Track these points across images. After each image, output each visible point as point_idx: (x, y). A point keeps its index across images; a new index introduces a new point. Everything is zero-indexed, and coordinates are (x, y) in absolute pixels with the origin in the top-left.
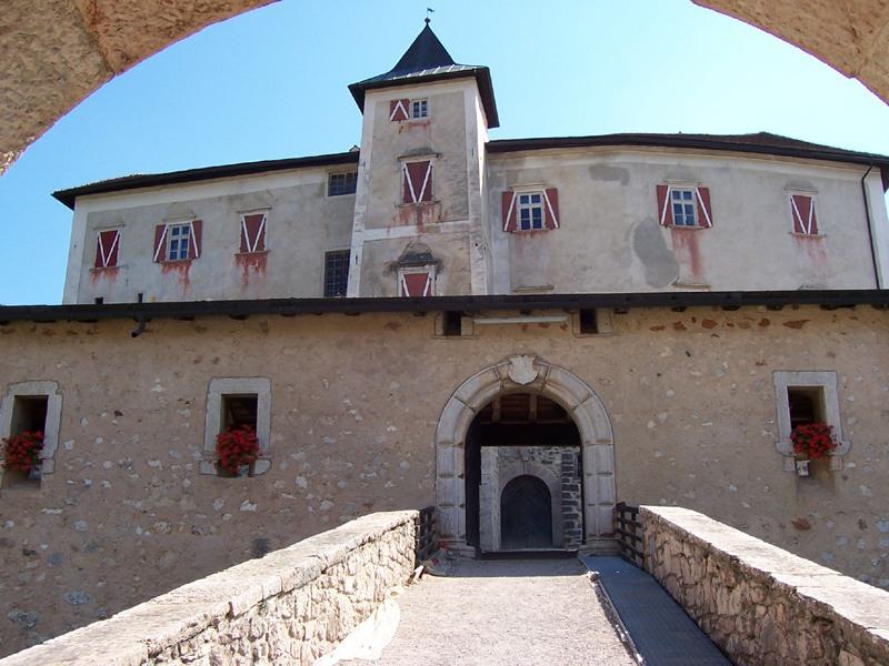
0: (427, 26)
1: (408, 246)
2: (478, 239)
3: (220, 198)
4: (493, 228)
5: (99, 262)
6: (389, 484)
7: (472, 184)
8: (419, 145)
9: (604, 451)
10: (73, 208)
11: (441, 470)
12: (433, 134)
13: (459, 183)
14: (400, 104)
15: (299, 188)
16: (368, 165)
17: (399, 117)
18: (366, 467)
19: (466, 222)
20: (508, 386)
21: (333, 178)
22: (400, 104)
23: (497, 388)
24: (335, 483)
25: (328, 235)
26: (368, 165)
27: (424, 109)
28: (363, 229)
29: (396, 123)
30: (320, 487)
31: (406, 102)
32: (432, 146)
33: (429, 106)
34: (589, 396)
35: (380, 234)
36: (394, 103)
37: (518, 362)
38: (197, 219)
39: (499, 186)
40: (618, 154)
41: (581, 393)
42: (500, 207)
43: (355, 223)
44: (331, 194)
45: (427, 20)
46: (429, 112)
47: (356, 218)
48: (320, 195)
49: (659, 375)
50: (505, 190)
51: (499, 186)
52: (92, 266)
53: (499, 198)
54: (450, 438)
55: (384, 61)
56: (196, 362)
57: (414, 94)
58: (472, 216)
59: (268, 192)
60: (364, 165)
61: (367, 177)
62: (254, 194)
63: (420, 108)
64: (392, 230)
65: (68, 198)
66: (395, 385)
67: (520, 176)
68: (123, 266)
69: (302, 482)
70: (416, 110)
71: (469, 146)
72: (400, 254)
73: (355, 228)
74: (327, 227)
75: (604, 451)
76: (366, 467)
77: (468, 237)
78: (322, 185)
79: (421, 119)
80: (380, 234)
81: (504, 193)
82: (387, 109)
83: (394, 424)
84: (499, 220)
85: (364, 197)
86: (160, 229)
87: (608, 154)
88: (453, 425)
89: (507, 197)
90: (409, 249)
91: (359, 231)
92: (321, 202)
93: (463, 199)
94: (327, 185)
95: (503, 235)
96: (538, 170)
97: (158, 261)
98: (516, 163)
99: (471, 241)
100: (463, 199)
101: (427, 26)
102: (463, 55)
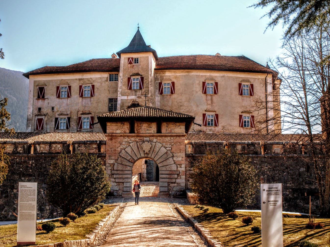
0: (138, 29)
1: (133, 101)
3: (76, 79)
7: (150, 85)
8: (136, 72)
13: (147, 84)
14: (131, 59)
16: (122, 77)
17: (130, 63)
22: (131, 59)
25: (109, 93)
29: (130, 65)
31: (132, 58)
35: (125, 98)
36: (129, 59)
40: (192, 72)
42: (158, 87)
43: (118, 94)
44: (110, 81)
45: (138, 27)
48: (107, 81)
50: (160, 81)
51: (158, 80)
53: (158, 84)
59: (91, 78)
61: (122, 81)
62: (87, 79)
64: (129, 97)
68: (47, 98)
72: (131, 104)
74: (109, 91)
77: (149, 100)
78: (107, 78)
81: (159, 83)
84: (158, 91)
85: (121, 86)
86: (58, 88)
89: (160, 84)
90: (133, 102)
91: (120, 96)
92: (107, 83)
93: (148, 89)
95: (159, 95)
98: (163, 73)
99: (150, 101)
100: (148, 89)
101: (138, 29)
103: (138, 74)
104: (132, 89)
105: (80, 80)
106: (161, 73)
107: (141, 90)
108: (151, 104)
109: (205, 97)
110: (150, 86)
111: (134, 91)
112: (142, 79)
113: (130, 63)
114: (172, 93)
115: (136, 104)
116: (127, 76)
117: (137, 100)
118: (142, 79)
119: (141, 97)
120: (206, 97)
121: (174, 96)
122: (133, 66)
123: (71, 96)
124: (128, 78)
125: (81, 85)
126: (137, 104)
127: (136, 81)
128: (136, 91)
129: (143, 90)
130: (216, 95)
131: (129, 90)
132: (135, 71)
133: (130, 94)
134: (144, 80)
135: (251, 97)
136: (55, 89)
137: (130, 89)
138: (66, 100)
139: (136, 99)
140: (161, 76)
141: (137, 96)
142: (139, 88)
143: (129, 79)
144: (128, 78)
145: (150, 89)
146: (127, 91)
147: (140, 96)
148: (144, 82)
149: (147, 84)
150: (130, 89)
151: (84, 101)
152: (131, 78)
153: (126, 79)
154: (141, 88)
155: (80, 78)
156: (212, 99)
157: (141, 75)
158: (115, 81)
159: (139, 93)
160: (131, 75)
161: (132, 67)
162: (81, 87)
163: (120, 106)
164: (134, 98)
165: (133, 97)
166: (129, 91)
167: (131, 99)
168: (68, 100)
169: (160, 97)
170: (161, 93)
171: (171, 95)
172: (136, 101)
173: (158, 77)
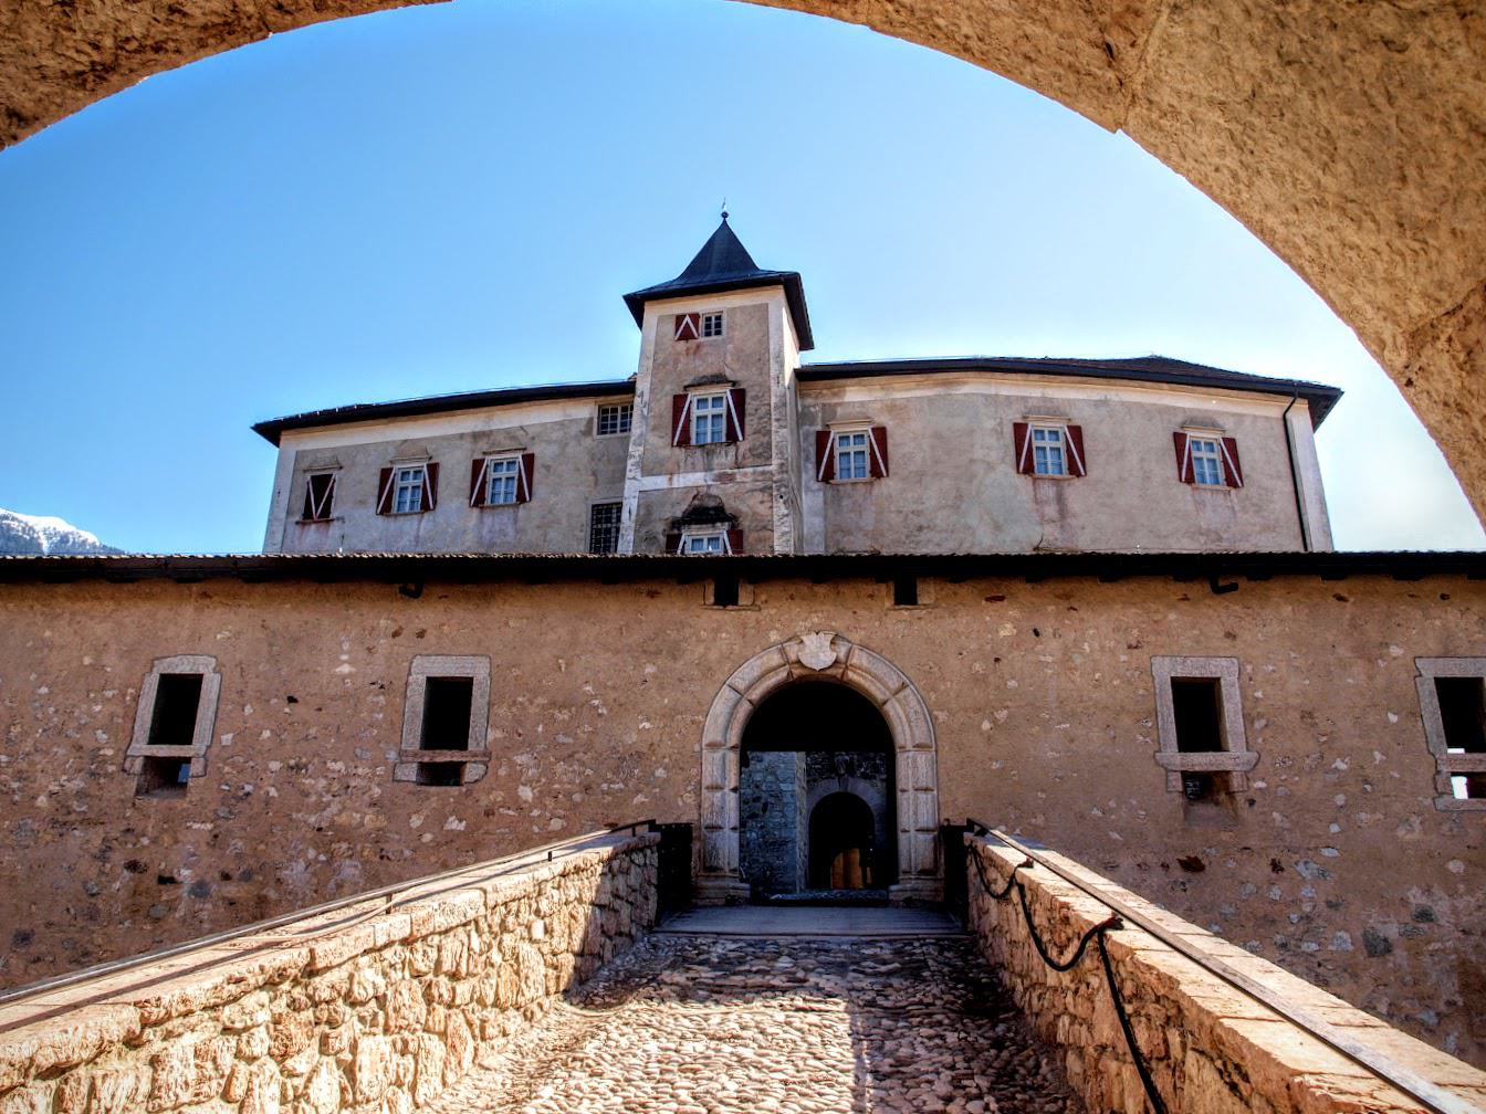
1: (694, 498)
2: (783, 489)
3: (462, 436)
4: (804, 475)
5: (307, 515)
6: (640, 798)
7: (777, 420)
8: (710, 371)
9: (923, 759)
10: (278, 446)
11: (706, 782)
12: (729, 358)
13: (760, 418)
14: (687, 319)
15: (561, 424)
16: (646, 398)
17: (686, 336)
18: (609, 776)
19: (770, 468)
20: (797, 672)
21: (603, 411)
22: (687, 319)
23: (782, 675)
24: (569, 794)
25: (596, 484)
26: (646, 398)
27: (718, 325)
28: (639, 476)
29: (682, 342)
30: (549, 802)
31: (695, 317)
32: (728, 373)
33: (724, 322)
34: (904, 686)
35: (661, 482)
36: (680, 318)
37: (811, 641)
38: (433, 461)
39: (811, 425)
41: (894, 683)
42: (813, 450)
43: (629, 468)
46: (724, 329)
47: (630, 462)
48: (587, 432)
49: (997, 660)
50: (819, 428)
52: (298, 518)
53: (812, 439)
54: (719, 738)
55: (671, 266)
56: (396, 634)
57: (705, 306)
58: (775, 462)
60: (642, 394)
63: (714, 325)
64: (675, 478)
65: (272, 431)
66: (650, 669)
67: (839, 410)
68: (338, 519)
69: (526, 793)
70: (708, 327)
71: (773, 373)
72: (684, 507)
73: (629, 474)
74: (594, 474)
75: (923, 759)
76: (609, 776)
78: (591, 420)
79: (714, 338)
80: (661, 482)
82: (671, 326)
83: (648, 720)
84: (811, 467)
85: (641, 435)
86: (385, 473)
87: (951, 383)
88: (723, 718)
89: (822, 437)
90: (696, 502)
91: (634, 478)
92: (588, 441)
94: (596, 420)
95: (816, 486)
96: (862, 404)
97: (381, 513)
98: (835, 395)
102: (766, 257)
103: (718, 379)
104: (693, 442)
105: (476, 436)
106: (825, 392)
107: (732, 450)
108: (783, 507)
109: (1030, 488)
110: (774, 424)
111: (699, 452)
112: (739, 396)
113: (686, 336)
114: (876, 473)
115: (708, 509)
116: (672, 389)
117: (714, 491)
118: (739, 396)
119: (730, 478)
120: (1035, 490)
121: (887, 486)
122: (698, 346)
123: (435, 502)
124: (675, 397)
125: (480, 457)
126: (715, 508)
127: (707, 410)
128: (707, 450)
129: (744, 446)
130: (1077, 482)
131: (677, 450)
132: (706, 367)
133: (682, 464)
134: (748, 400)
135: (1233, 491)
136: (376, 481)
137: (684, 442)
138: (416, 523)
139: (709, 486)
140: (824, 405)
141: (716, 472)
142: (724, 440)
143: (679, 401)
144: (675, 397)
145: (775, 439)
146: (667, 452)
147: (729, 471)
148: (749, 408)
149: (760, 418)
150: (684, 442)
151: (488, 519)
152: (686, 396)
153: (666, 404)
154: (732, 438)
155: (477, 430)
156: (1060, 499)
157: (734, 383)
158: (622, 431)
159: (724, 459)
160: (686, 383)
161: (695, 353)
162: (477, 465)
163: (636, 521)
164: (702, 483)
165: (695, 479)
166: (680, 453)
167: (687, 489)
168: (423, 524)
169: (821, 494)
170: (828, 477)
171: (871, 483)
172: (710, 496)
173: (812, 409)
